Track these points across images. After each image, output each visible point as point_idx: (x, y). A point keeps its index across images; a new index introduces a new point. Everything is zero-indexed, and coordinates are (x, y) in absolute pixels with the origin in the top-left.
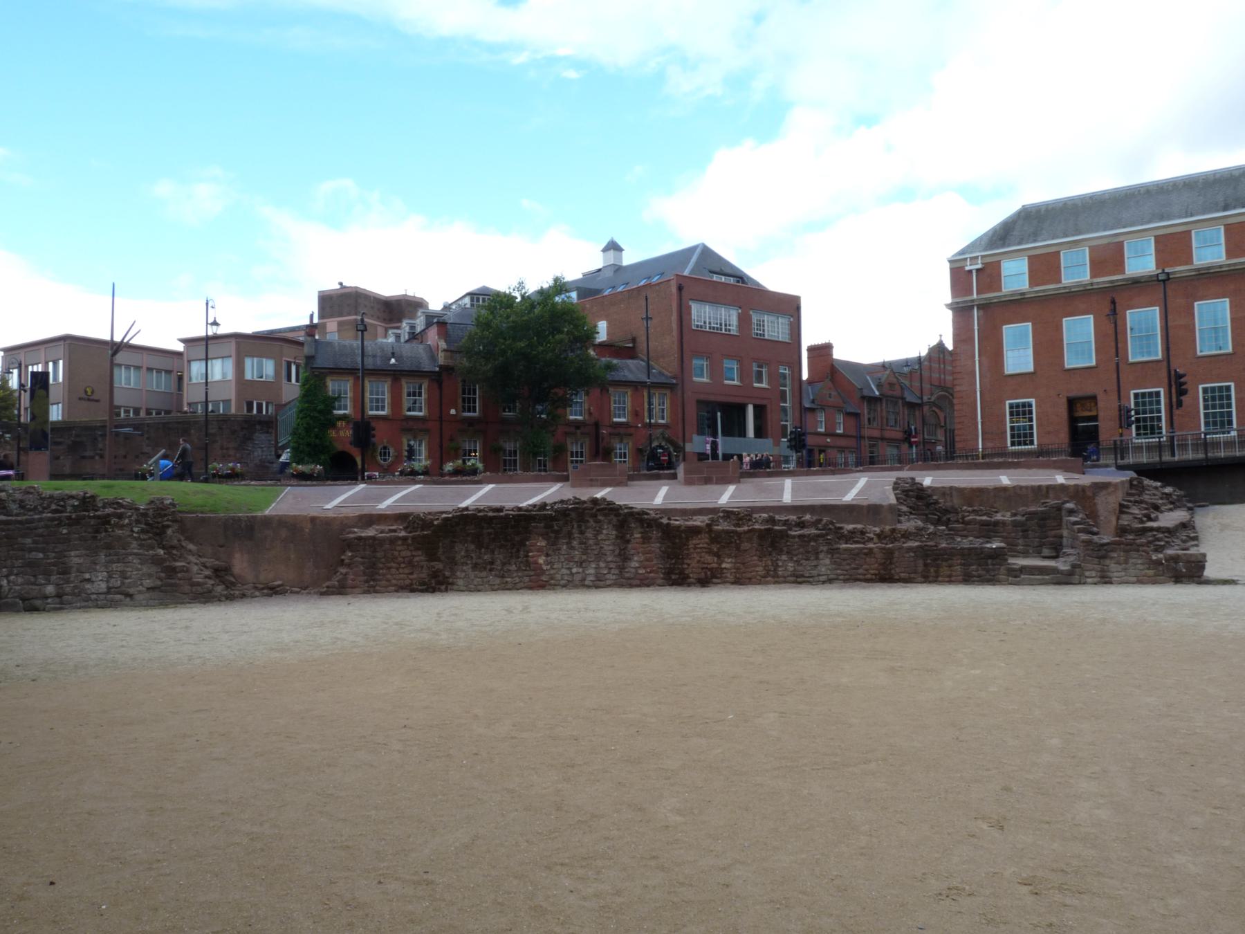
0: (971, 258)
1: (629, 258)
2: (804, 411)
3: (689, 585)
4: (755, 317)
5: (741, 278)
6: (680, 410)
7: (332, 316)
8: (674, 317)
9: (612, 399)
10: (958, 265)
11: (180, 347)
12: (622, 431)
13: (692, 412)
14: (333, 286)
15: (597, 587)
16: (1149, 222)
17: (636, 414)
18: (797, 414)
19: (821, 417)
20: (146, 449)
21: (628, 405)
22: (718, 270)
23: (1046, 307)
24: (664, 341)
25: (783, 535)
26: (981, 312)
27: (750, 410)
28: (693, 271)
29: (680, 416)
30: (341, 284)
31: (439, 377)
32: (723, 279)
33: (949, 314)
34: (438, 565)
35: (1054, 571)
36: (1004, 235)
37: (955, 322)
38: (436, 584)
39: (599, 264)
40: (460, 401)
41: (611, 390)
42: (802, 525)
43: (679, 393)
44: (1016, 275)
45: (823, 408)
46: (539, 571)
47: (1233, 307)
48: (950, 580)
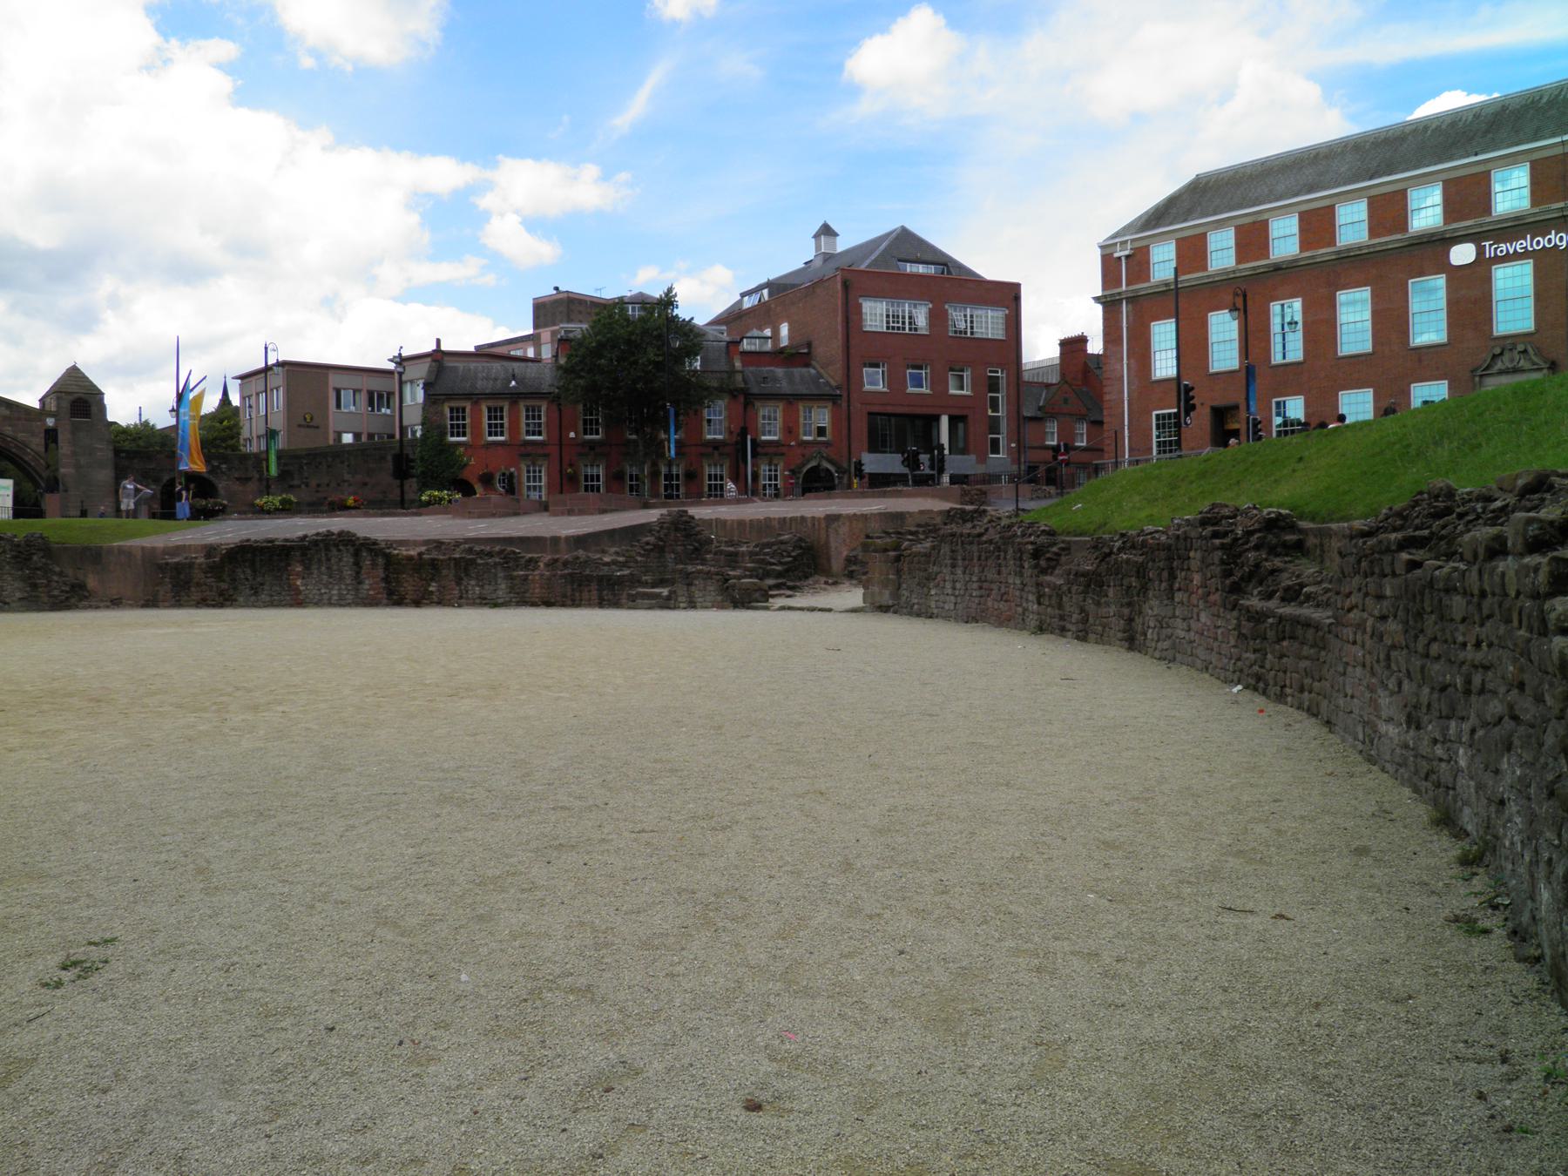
1: (842, 244)
2: (1020, 422)
3: (407, 605)
7: (546, 325)
8: (839, 319)
9: (761, 413)
10: (1108, 251)
11: (391, 366)
12: (771, 450)
13: (860, 427)
14: (547, 291)
15: (341, 606)
16: (1296, 195)
17: (790, 430)
19: (1053, 427)
20: (347, 477)
21: (779, 423)
22: (912, 257)
23: (1187, 301)
24: (829, 348)
25: (473, 562)
27: (945, 420)
29: (845, 432)
30: (556, 288)
31: (554, 399)
32: (921, 269)
33: (1099, 308)
34: (224, 586)
35: (658, 596)
36: (1159, 216)
38: (224, 600)
39: (810, 254)
40: (581, 423)
41: (758, 404)
42: (490, 555)
43: (844, 405)
44: (1163, 261)
46: (299, 592)
47: (1375, 297)
48: (590, 605)
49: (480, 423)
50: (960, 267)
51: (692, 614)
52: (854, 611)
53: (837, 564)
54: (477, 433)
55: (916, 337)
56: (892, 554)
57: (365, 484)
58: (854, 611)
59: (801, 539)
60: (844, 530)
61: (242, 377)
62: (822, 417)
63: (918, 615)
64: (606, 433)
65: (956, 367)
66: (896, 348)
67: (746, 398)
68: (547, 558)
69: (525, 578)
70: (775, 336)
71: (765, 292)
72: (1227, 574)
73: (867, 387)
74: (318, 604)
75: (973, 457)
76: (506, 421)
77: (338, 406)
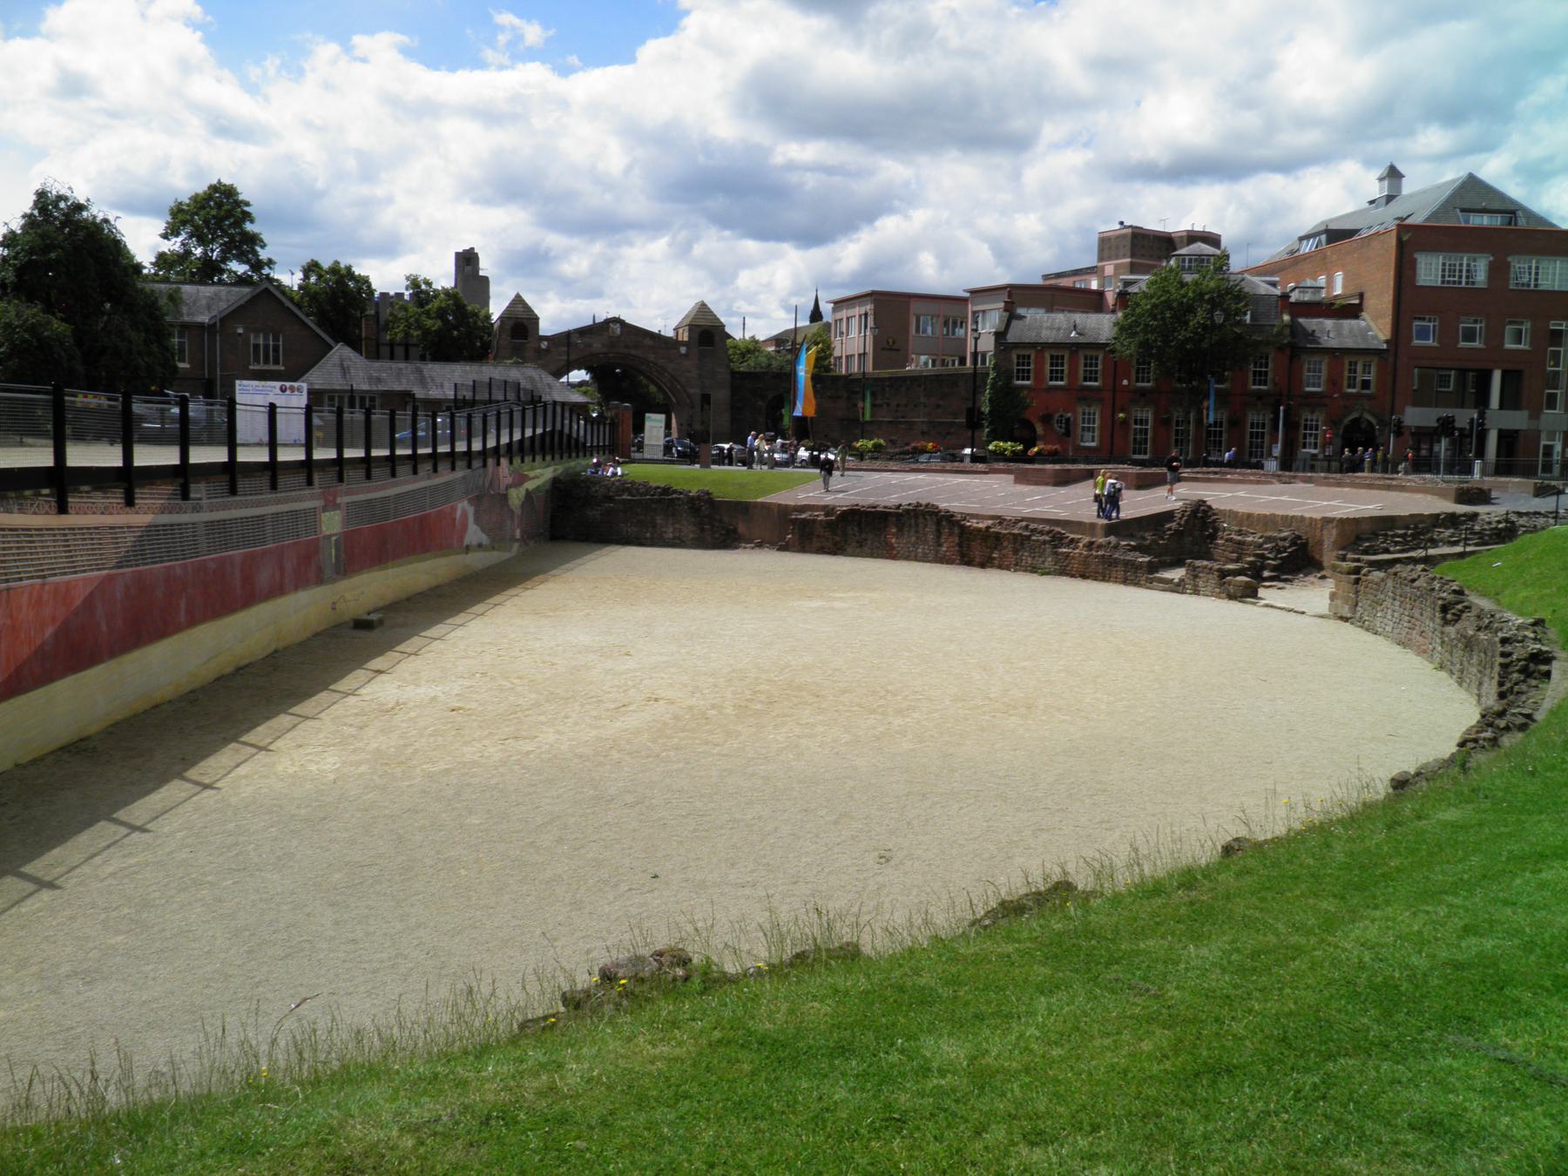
5: (1511, 210)
7: (1109, 258)
17: (1334, 382)
21: (1324, 374)
25: (1028, 537)
27: (1497, 376)
28: (1434, 215)
38: (836, 549)
42: (1042, 533)
43: (1391, 360)
51: (1194, 597)
54: (1039, 378)
57: (938, 406)
59: (1299, 537)
63: (1367, 630)
66: (1450, 302)
68: (1086, 539)
69: (1067, 555)
70: (1330, 281)
71: (1323, 237)
72: (1501, 684)
73: (1416, 342)
74: (907, 558)
75: (1525, 413)
76: (1066, 367)
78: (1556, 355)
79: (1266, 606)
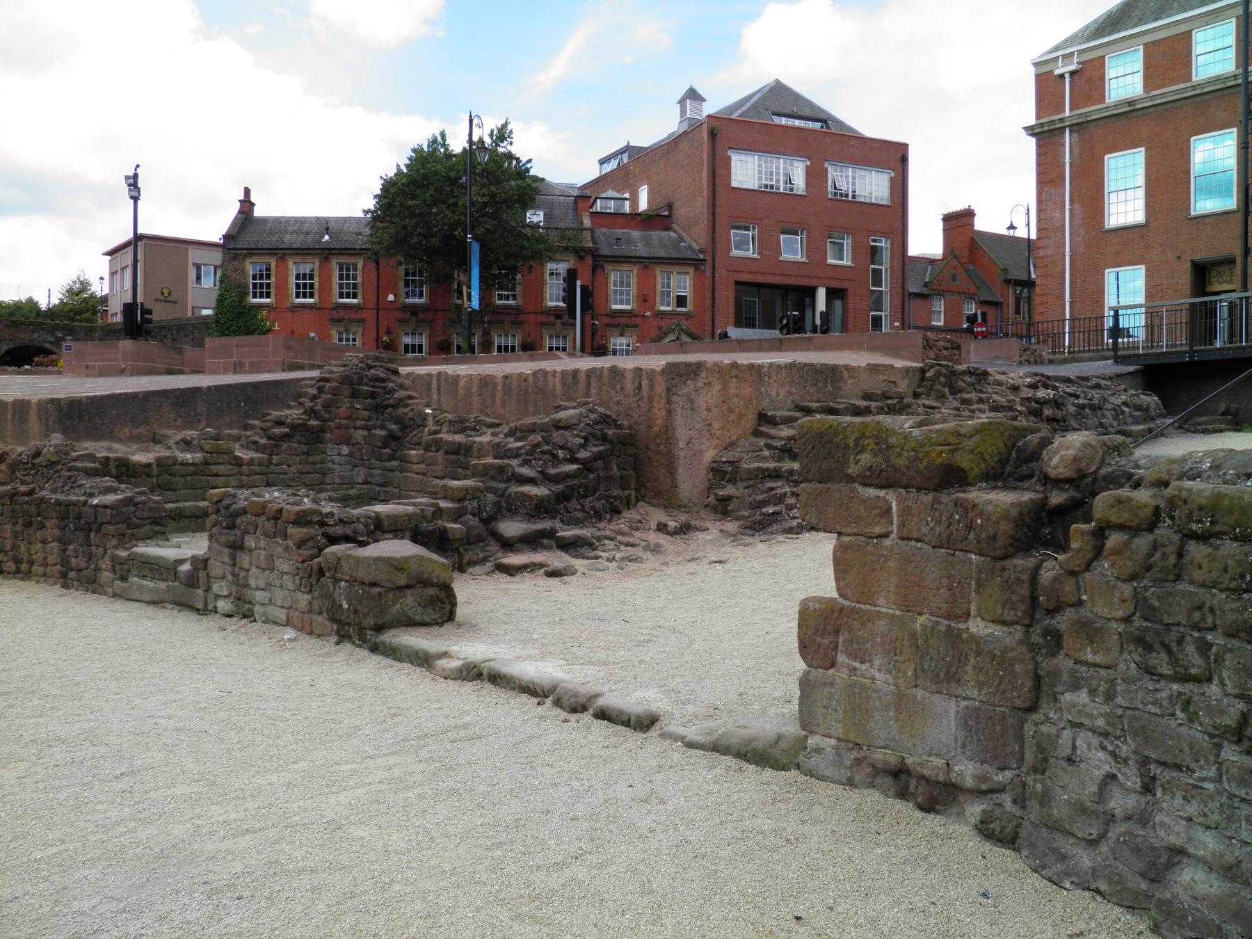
0: (1064, 57)
1: (709, 108)
2: (905, 297)
4: (832, 172)
5: (825, 119)
6: (708, 294)
8: (705, 174)
12: (623, 321)
13: (726, 297)
17: (645, 298)
18: (898, 302)
19: (939, 306)
26: (1075, 136)
27: (821, 294)
28: (745, 113)
29: (708, 302)
32: (797, 123)
33: (1032, 141)
37: (1040, 155)
40: (402, 284)
41: (608, 267)
43: (708, 271)
44: (1125, 79)
45: (940, 293)
49: (286, 281)
50: (841, 124)
52: (757, 755)
53: (690, 480)
55: (790, 196)
56: (1001, 500)
58: (757, 755)
59: (605, 420)
60: (708, 398)
61: (110, 253)
62: (683, 283)
64: (432, 295)
65: (833, 231)
66: (769, 208)
67: (598, 260)
70: (634, 200)
73: (735, 253)
77: (199, 278)
78: (877, 274)
79: (473, 673)
